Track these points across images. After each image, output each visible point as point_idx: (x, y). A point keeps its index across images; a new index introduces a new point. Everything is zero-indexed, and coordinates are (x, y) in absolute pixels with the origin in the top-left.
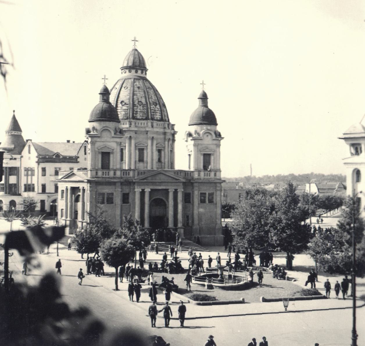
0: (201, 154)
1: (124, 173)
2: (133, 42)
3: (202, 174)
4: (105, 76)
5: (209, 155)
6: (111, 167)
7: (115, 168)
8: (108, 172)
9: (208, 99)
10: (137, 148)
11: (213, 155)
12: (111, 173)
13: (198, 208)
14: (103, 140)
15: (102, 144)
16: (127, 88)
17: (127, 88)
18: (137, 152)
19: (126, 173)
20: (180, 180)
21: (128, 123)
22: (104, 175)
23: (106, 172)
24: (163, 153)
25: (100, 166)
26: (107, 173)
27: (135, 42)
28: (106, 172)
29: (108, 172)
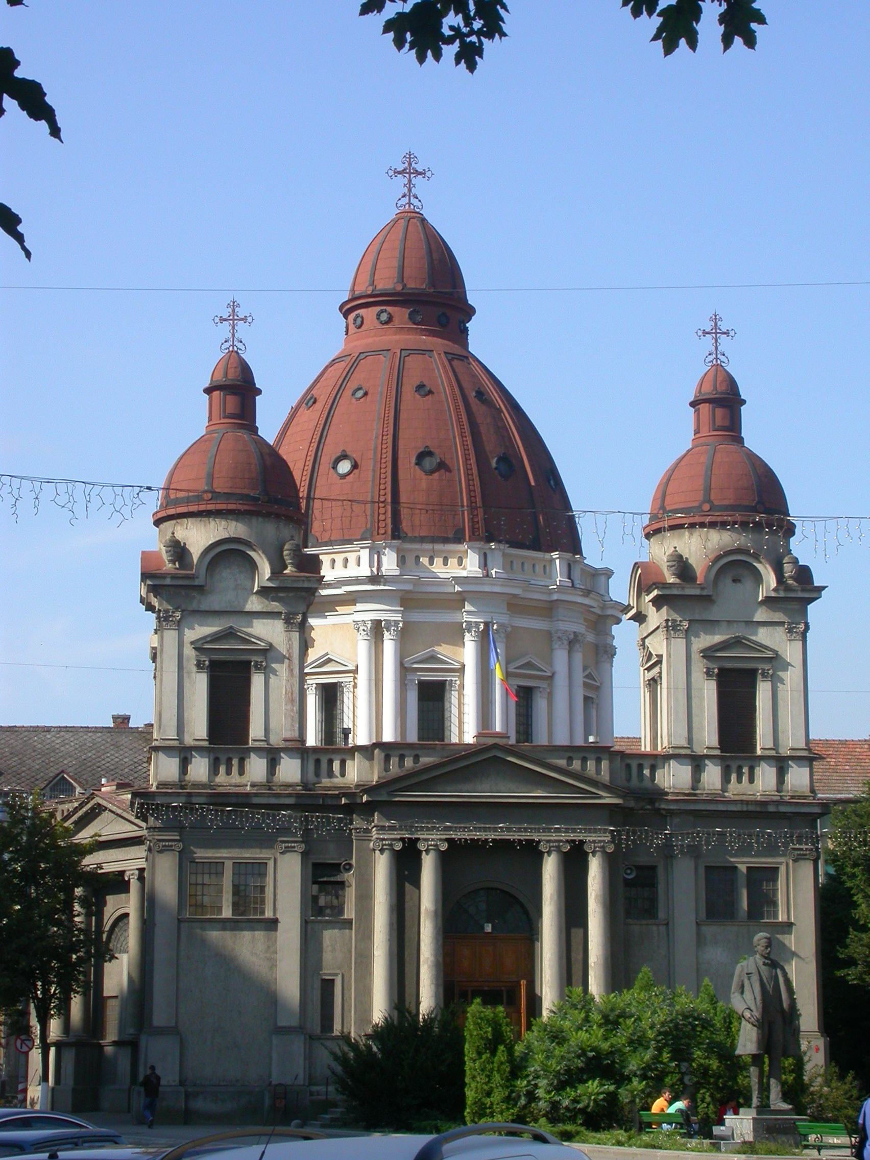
0: (709, 673)
1: (318, 762)
2: (402, 180)
6: (256, 730)
7: (276, 740)
9: (744, 402)
10: (416, 678)
12: (257, 768)
13: (700, 941)
14: (214, 602)
16: (366, 394)
18: (413, 697)
20: (600, 797)
21: (365, 554)
24: (540, 704)
27: (410, 181)
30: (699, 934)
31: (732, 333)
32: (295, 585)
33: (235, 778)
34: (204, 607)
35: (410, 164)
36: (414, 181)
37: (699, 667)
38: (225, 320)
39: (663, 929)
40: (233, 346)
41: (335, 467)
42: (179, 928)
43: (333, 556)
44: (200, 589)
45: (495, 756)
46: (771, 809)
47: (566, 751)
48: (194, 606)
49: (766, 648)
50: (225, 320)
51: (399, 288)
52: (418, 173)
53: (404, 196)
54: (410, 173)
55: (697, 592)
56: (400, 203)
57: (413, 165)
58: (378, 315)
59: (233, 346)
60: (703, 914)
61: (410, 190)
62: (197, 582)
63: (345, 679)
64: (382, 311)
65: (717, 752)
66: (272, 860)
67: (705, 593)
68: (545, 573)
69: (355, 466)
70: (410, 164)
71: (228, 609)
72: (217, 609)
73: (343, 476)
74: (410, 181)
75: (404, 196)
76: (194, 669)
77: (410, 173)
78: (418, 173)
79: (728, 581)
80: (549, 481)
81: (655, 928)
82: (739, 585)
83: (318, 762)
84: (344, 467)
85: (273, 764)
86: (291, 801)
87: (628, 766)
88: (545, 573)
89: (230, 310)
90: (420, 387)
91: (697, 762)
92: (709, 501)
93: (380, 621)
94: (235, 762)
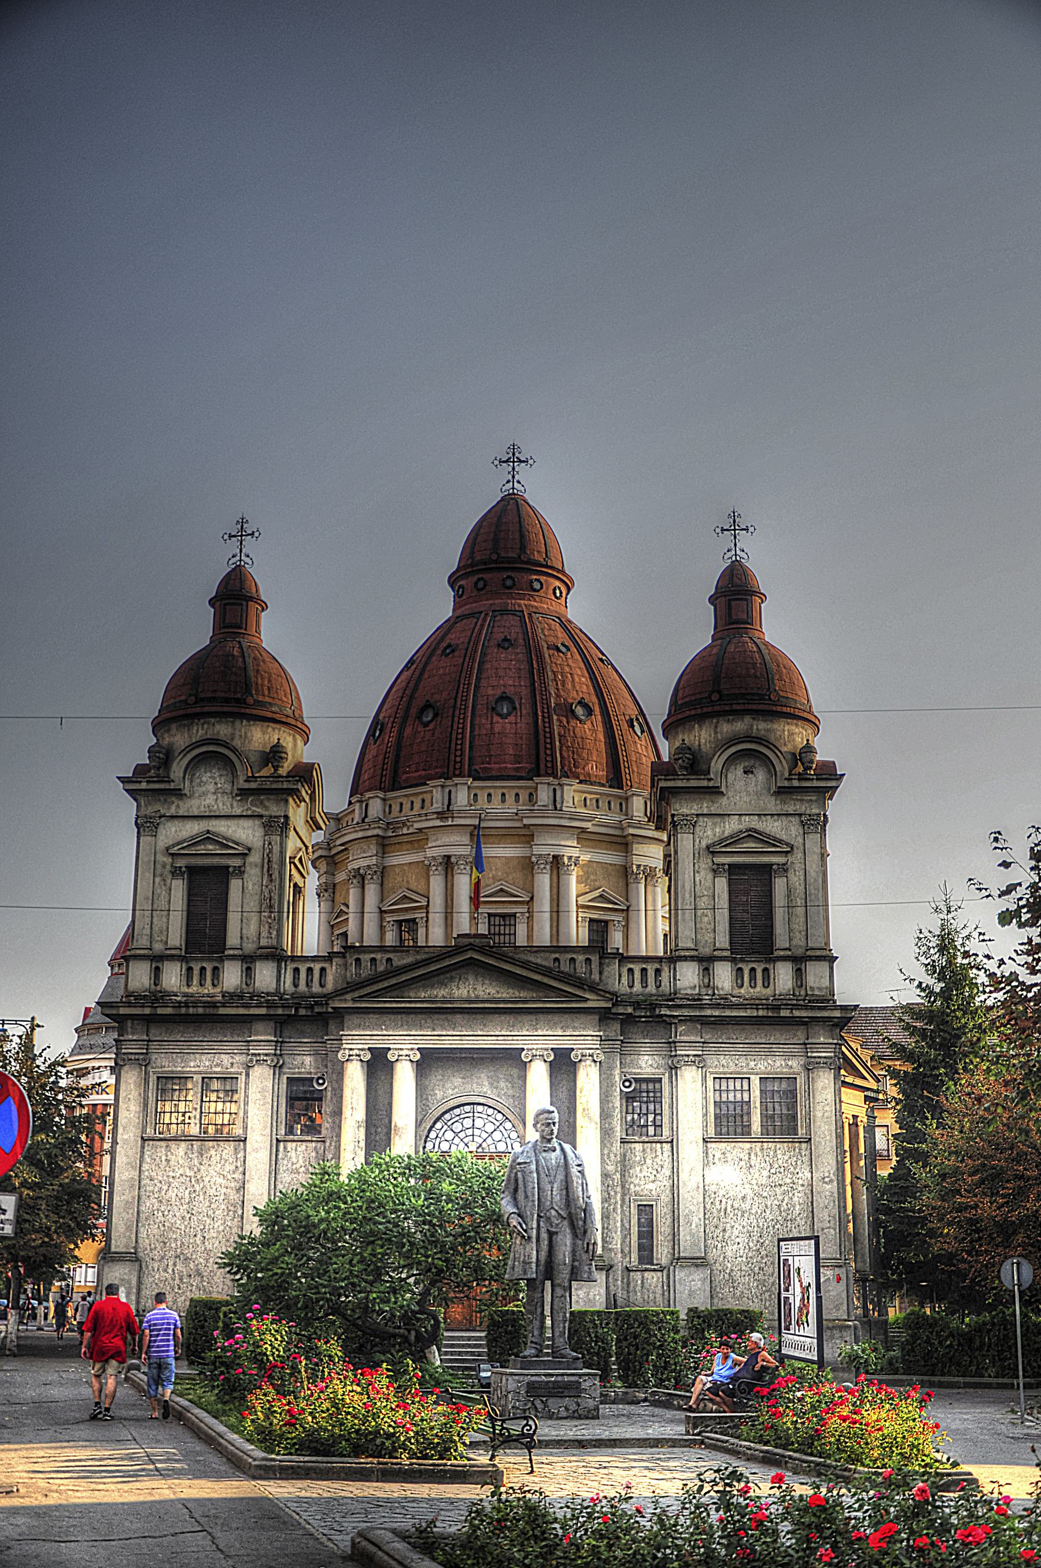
0: (715, 871)
1: (296, 970)
3: (724, 976)
4: (242, 522)
5: (766, 872)
6: (233, 939)
7: (249, 947)
8: (215, 969)
11: (784, 869)
12: (232, 977)
14: (194, 806)
15: (192, 829)
17: (453, 651)
19: (310, 970)
22: (195, 981)
23: (203, 969)
25: (176, 937)
26: (209, 974)
27: (514, 469)
28: (203, 969)
29: (215, 969)
30: (706, 1153)
31: (751, 529)
32: (274, 786)
33: (208, 989)
34: (181, 813)
35: (514, 454)
36: (517, 469)
37: (705, 863)
38: (234, 536)
39: (667, 1147)
40: (240, 560)
41: (419, 717)
42: (143, 1147)
43: (411, 798)
44: (178, 793)
45: (471, 958)
46: (784, 1013)
47: (551, 952)
48: (173, 811)
49: (780, 841)
50: (234, 536)
51: (494, 557)
52: (521, 461)
53: (508, 482)
54: (514, 462)
55: (705, 783)
56: (504, 488)
57: (517, 454)
58: (476, 584)
59: (240, 560)
60: (711, 1132)
61: (513, 477)
62: (172, 786)
63: (419, 915)
64: (479, 579)
65: (727, 954)
66: (244, 1074)
67: (711, 784)
68: (621, 810)
69: (436, 715)
70: (514, 454)
71: (207, 814)
72: (196, 814)
73: (426, 724)
74: (514, 469)
75: (508, 482)
76: (170, 876)
77: (514, 462)
78: (521, 461)
79: (739, 772)
80: (633, 727)
81: (659, 1145)
82: (750, 776)
83: (296, 970)
84: (428, 717)
85: (249, 972)
86: (263, 1011)
87: (630, 971)
88: (621, 810)
89: (239, 526)
90: (505, 640)
91: (706, 962)
92: (719, 692)
93: (449, 857)
94: (209, 974)
